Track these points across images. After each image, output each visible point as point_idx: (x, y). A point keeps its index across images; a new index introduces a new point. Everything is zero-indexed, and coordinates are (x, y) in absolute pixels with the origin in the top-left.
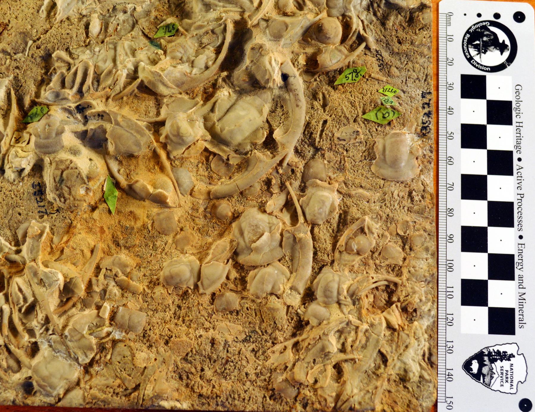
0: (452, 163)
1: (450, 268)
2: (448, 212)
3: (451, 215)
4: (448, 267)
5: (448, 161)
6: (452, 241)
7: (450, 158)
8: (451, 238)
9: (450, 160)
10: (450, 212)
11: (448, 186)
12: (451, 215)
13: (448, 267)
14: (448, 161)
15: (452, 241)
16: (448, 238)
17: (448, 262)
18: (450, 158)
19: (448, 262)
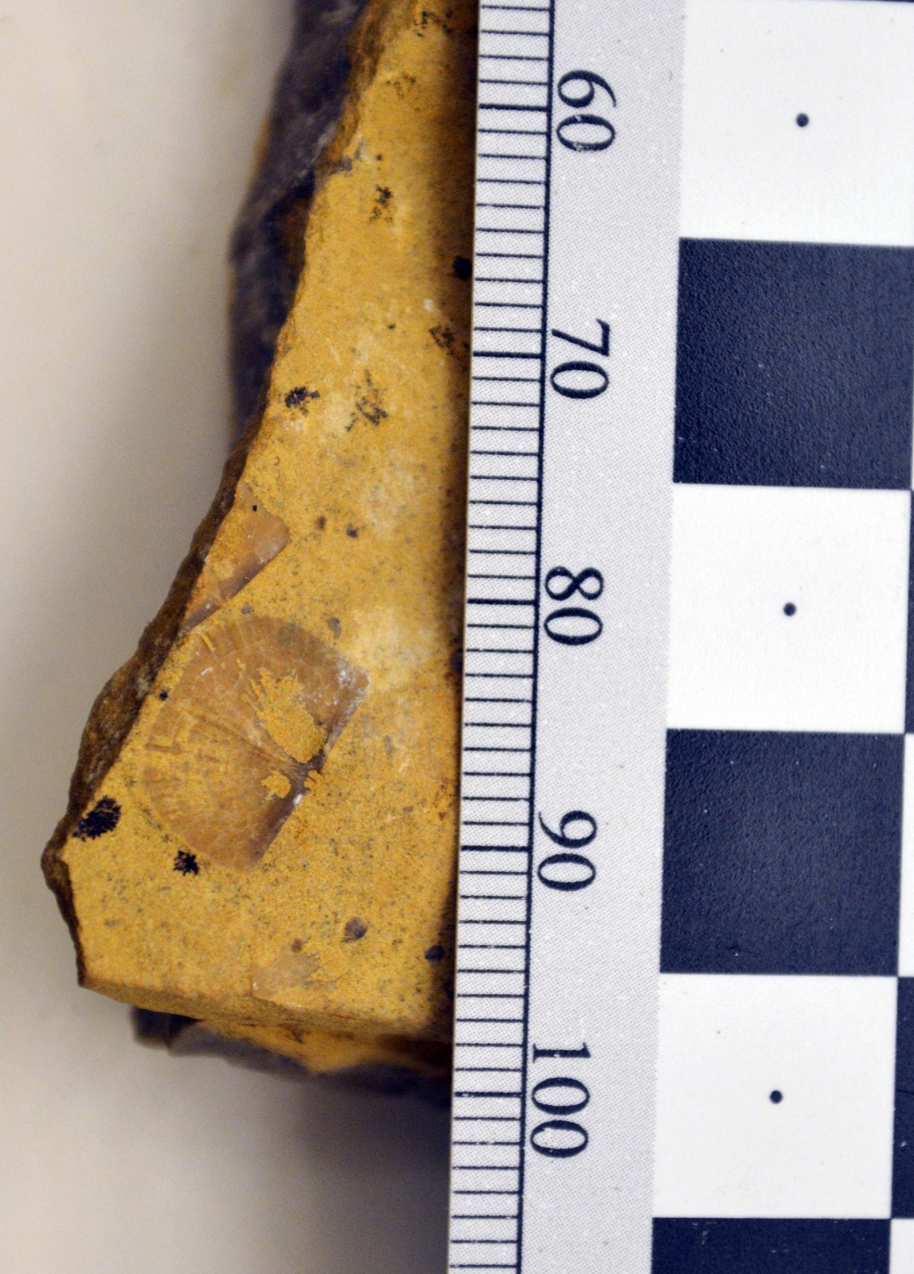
0: (599, 134)
1: (557, 1120)
2: (548, 606)
3: (584, 627)
4: (535, 1117)
5: (562, 111)
6: (578, 873)
7: (577, 89)
8: (571, 849)
9: (578, 106)
10: (569, 599)
11: (560, 353)
12: (584, 627)
13: (535, 1117)
14: (562, 111)
15: (578, 873)
16: (545, 847)
17: (540, 1070)
18: (577, 89)
19: (540, 1070)
